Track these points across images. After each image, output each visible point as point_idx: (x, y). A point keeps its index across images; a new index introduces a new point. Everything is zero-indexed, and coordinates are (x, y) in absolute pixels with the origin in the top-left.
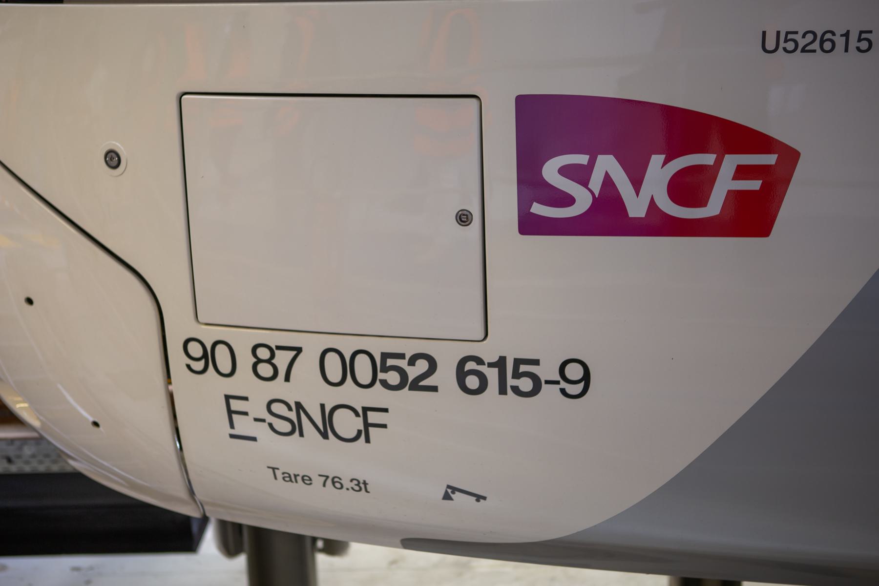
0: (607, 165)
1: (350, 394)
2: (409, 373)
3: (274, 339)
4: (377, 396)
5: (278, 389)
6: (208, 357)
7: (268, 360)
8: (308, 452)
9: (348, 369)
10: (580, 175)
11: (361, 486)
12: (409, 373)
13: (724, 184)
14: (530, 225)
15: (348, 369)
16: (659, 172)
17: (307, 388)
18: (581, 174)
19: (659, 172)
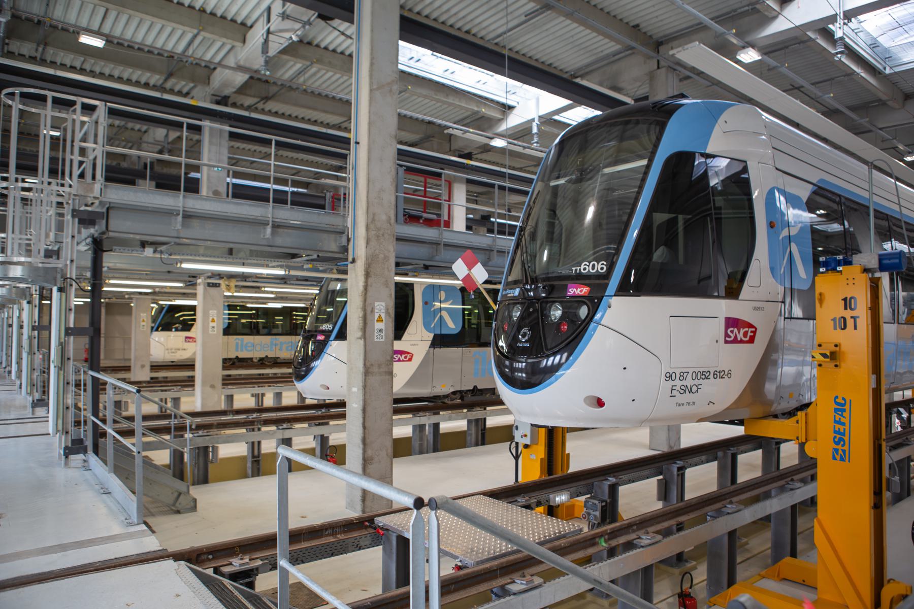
0: (736, 330)
1: (697, 382)
2: (705, 375)
3: (684, 370)
4: (701, 381)
5: (684, 383)
6: (670, 377)
7: (682, 376)
8: (688, 397)
9: (697, 376)
10: (735, 332)
11: (694, 403)
12: (705, 375)
13: (750, 334)
14: (726, 342)
15: (697, 376)
16: (742, 331)
17: (689, 382)
18: (732, 332)
19: (742, 331)
